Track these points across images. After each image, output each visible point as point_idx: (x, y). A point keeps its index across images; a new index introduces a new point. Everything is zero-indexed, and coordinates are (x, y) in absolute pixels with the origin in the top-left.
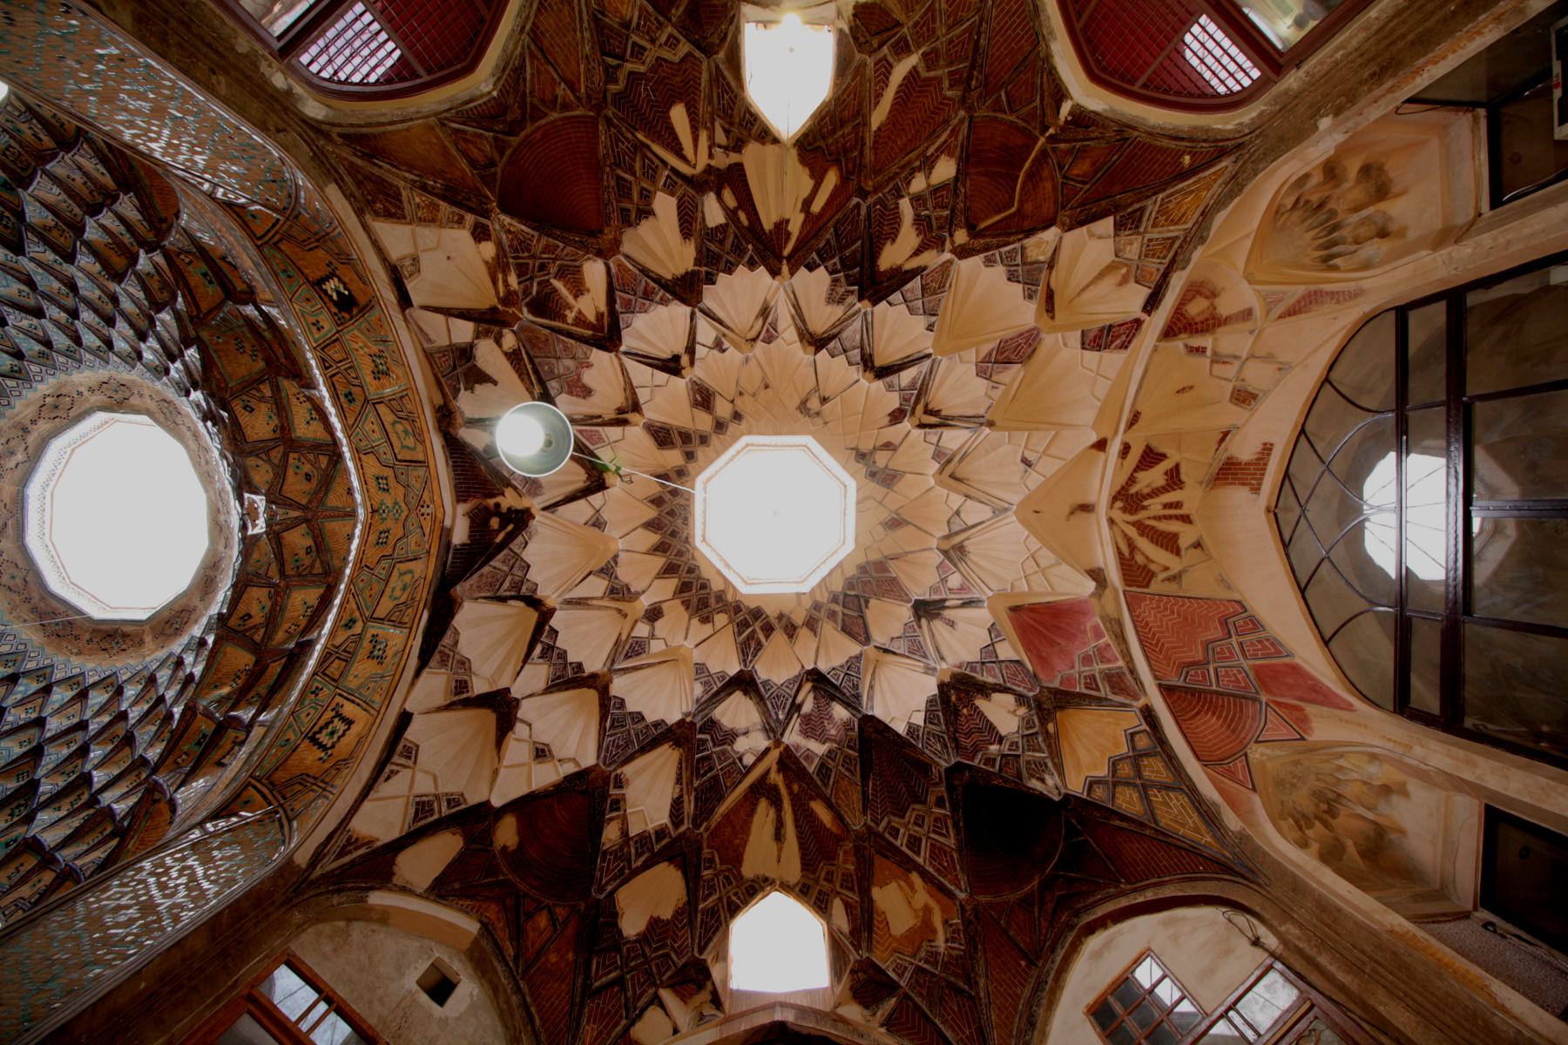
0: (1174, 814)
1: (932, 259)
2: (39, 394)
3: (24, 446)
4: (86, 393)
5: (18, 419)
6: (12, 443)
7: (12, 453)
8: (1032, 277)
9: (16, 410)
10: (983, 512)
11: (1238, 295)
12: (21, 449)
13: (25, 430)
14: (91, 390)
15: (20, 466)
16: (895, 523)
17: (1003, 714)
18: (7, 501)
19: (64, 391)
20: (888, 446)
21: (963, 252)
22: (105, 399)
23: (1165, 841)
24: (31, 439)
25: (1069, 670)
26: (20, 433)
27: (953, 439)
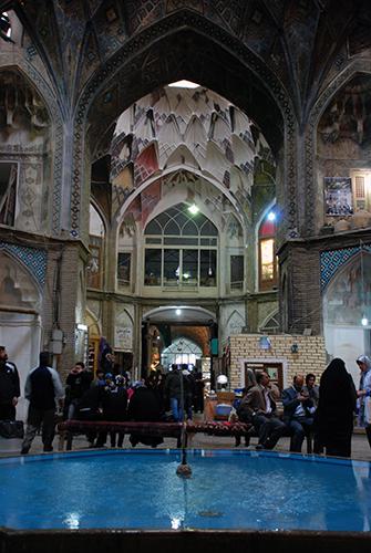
0: (115, 205)
1: (258, 149)
8: (244, 169)
10: (182, 132)
11: (229, 211)
16: (179, 98)
17: (124, 154)
20: (207, 100)
21: (256, 158)
23: (110, 208)
25: (138, 166)
27: (207, 125)
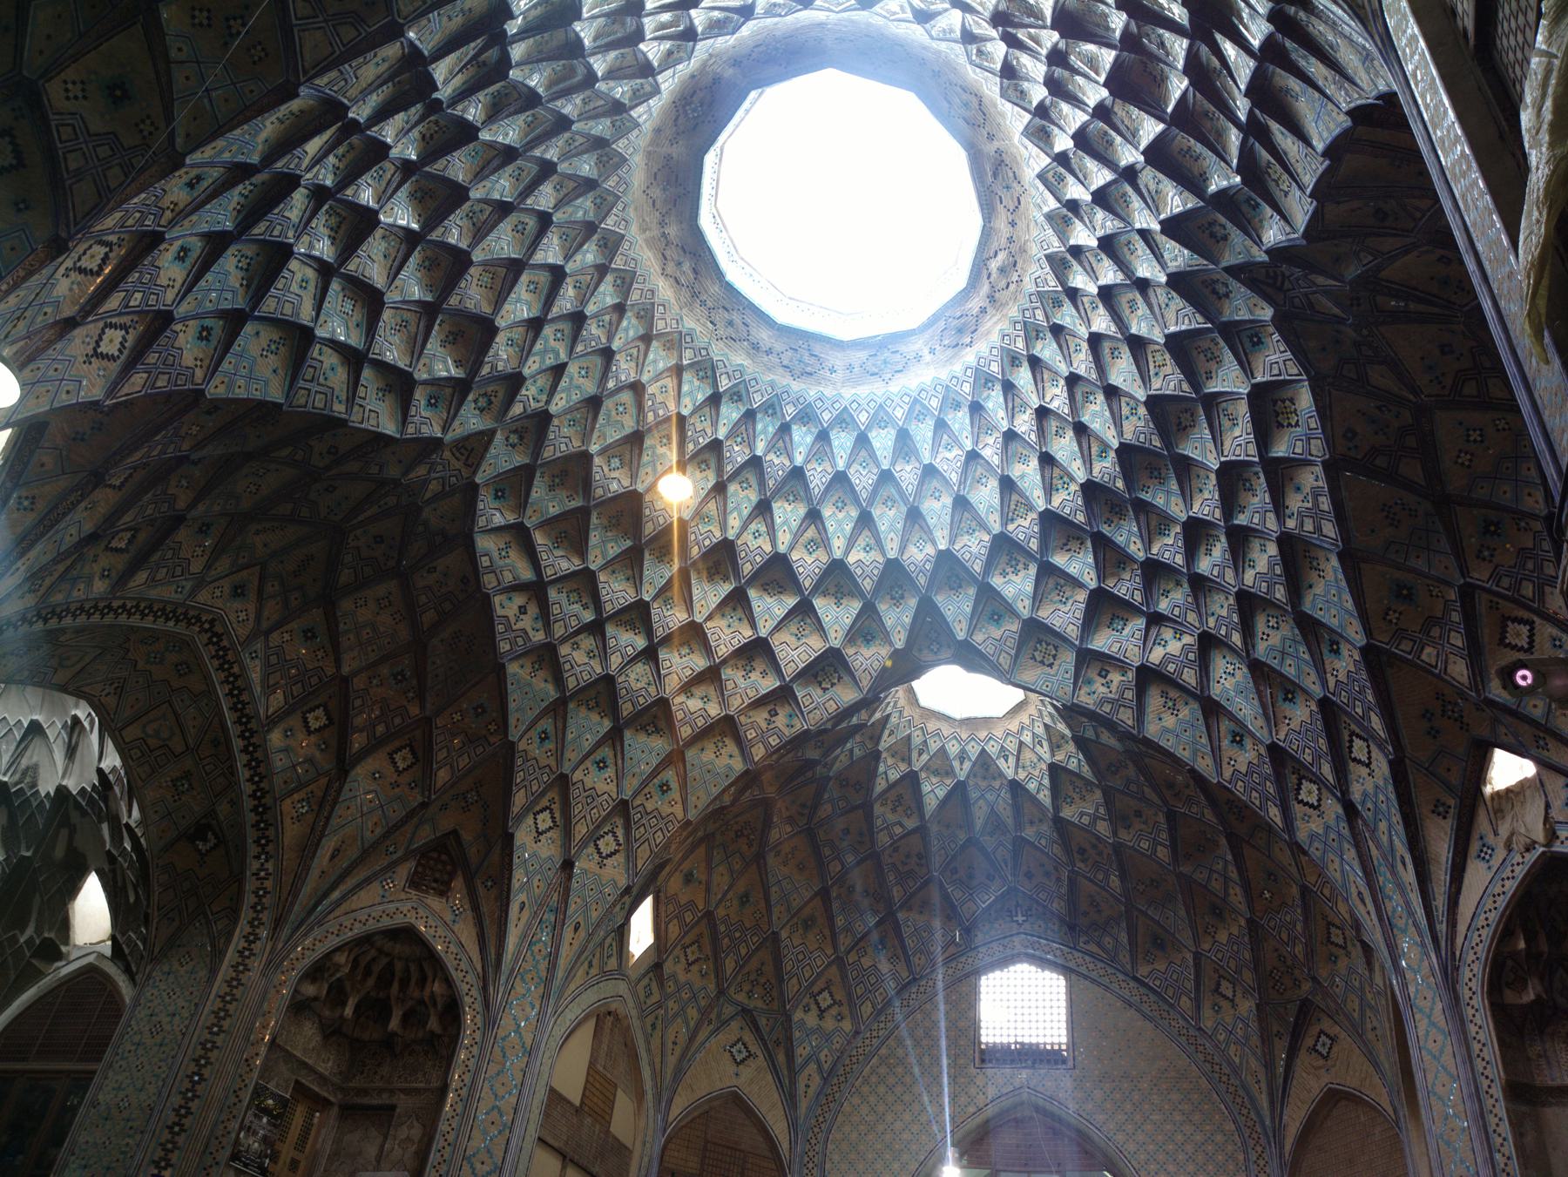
2: (976, 347)
3: (992, 279)
4: (926, 351)
6: (1003, 284)
7: (1002, 270)
9: (999, 327)
13: (992, 298)
14: (918, 358)
18: (1000, 208)
19: (950, 352)
22: (903, 348)
24: (985, 289)
26: (997, 295)
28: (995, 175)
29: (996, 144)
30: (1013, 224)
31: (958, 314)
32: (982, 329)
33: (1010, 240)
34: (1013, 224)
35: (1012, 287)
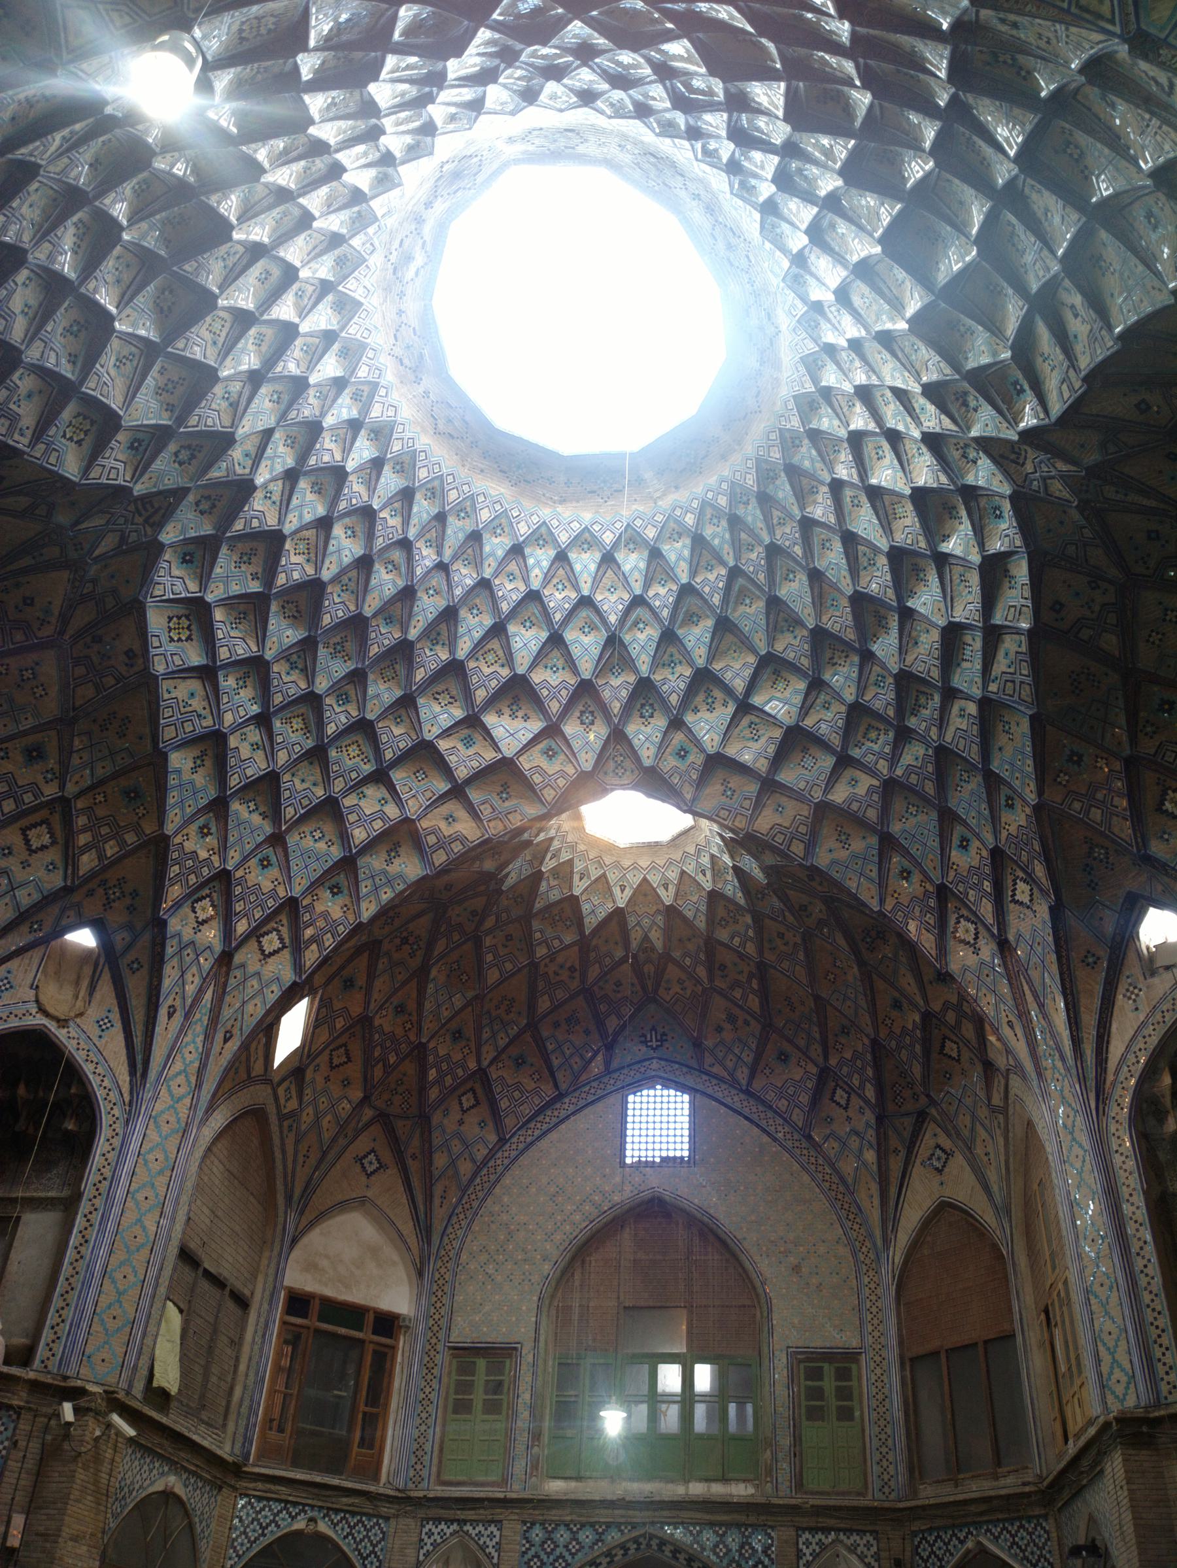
3: (420, 242)
5: (409, 208)
7: (408, 258)
12: (418, 248)
13: (419, 220)
15: (422, 272)
28: (421, 356)
29: (421, 390)
30: (400, 313)
31: (459, 194)
32: (429, 185)
33: (402, 295)
34: (400, 313)
35: (396, 244)
